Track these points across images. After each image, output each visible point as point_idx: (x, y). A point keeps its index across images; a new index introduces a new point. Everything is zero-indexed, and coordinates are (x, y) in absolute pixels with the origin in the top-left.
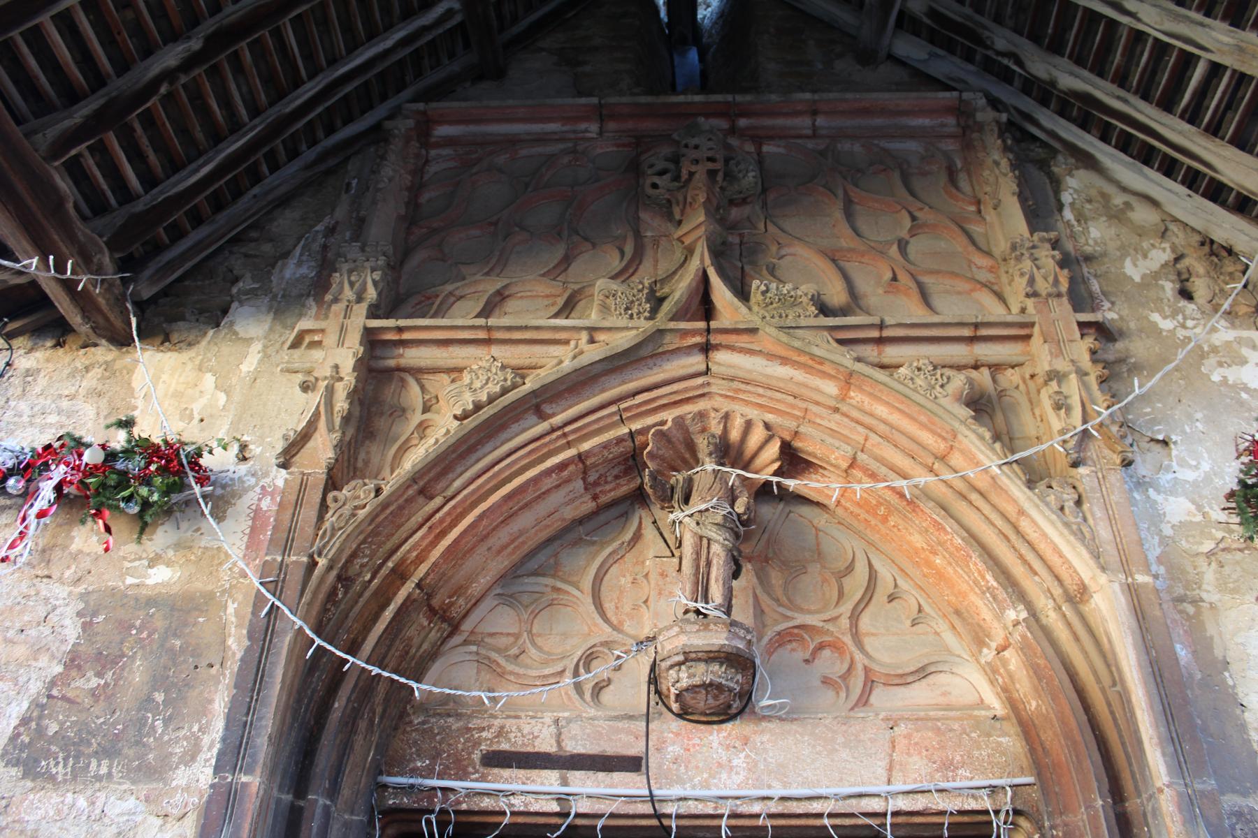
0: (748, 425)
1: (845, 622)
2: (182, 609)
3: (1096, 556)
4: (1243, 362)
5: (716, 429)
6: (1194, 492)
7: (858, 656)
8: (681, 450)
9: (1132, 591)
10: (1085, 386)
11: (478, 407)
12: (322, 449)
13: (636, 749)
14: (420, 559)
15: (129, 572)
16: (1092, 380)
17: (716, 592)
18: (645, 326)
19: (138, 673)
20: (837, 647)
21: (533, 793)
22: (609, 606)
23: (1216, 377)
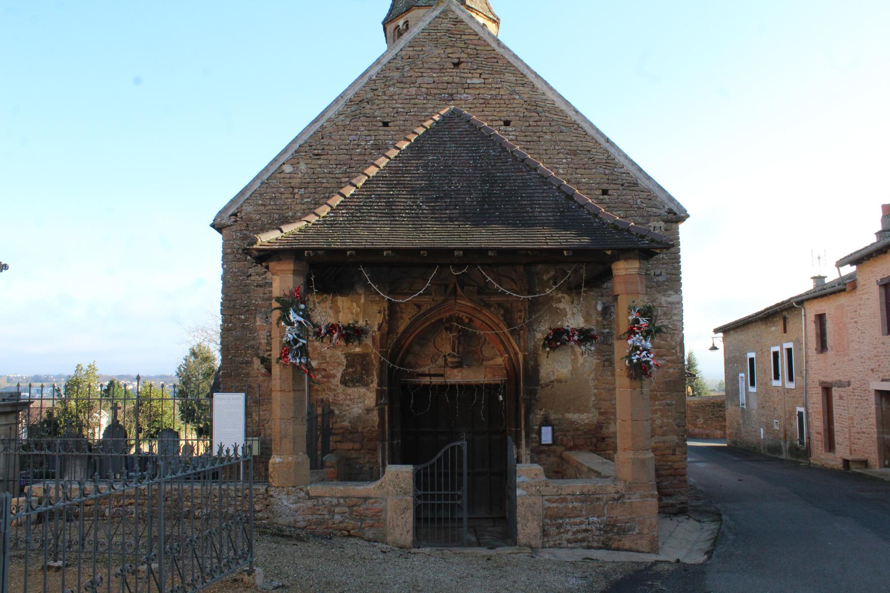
2: (364, 356)
4: (560, 302)
8: (450, 319)
12: (386, 328)
13: (442, 372)
19: (359, 368)
21: (426, 380)
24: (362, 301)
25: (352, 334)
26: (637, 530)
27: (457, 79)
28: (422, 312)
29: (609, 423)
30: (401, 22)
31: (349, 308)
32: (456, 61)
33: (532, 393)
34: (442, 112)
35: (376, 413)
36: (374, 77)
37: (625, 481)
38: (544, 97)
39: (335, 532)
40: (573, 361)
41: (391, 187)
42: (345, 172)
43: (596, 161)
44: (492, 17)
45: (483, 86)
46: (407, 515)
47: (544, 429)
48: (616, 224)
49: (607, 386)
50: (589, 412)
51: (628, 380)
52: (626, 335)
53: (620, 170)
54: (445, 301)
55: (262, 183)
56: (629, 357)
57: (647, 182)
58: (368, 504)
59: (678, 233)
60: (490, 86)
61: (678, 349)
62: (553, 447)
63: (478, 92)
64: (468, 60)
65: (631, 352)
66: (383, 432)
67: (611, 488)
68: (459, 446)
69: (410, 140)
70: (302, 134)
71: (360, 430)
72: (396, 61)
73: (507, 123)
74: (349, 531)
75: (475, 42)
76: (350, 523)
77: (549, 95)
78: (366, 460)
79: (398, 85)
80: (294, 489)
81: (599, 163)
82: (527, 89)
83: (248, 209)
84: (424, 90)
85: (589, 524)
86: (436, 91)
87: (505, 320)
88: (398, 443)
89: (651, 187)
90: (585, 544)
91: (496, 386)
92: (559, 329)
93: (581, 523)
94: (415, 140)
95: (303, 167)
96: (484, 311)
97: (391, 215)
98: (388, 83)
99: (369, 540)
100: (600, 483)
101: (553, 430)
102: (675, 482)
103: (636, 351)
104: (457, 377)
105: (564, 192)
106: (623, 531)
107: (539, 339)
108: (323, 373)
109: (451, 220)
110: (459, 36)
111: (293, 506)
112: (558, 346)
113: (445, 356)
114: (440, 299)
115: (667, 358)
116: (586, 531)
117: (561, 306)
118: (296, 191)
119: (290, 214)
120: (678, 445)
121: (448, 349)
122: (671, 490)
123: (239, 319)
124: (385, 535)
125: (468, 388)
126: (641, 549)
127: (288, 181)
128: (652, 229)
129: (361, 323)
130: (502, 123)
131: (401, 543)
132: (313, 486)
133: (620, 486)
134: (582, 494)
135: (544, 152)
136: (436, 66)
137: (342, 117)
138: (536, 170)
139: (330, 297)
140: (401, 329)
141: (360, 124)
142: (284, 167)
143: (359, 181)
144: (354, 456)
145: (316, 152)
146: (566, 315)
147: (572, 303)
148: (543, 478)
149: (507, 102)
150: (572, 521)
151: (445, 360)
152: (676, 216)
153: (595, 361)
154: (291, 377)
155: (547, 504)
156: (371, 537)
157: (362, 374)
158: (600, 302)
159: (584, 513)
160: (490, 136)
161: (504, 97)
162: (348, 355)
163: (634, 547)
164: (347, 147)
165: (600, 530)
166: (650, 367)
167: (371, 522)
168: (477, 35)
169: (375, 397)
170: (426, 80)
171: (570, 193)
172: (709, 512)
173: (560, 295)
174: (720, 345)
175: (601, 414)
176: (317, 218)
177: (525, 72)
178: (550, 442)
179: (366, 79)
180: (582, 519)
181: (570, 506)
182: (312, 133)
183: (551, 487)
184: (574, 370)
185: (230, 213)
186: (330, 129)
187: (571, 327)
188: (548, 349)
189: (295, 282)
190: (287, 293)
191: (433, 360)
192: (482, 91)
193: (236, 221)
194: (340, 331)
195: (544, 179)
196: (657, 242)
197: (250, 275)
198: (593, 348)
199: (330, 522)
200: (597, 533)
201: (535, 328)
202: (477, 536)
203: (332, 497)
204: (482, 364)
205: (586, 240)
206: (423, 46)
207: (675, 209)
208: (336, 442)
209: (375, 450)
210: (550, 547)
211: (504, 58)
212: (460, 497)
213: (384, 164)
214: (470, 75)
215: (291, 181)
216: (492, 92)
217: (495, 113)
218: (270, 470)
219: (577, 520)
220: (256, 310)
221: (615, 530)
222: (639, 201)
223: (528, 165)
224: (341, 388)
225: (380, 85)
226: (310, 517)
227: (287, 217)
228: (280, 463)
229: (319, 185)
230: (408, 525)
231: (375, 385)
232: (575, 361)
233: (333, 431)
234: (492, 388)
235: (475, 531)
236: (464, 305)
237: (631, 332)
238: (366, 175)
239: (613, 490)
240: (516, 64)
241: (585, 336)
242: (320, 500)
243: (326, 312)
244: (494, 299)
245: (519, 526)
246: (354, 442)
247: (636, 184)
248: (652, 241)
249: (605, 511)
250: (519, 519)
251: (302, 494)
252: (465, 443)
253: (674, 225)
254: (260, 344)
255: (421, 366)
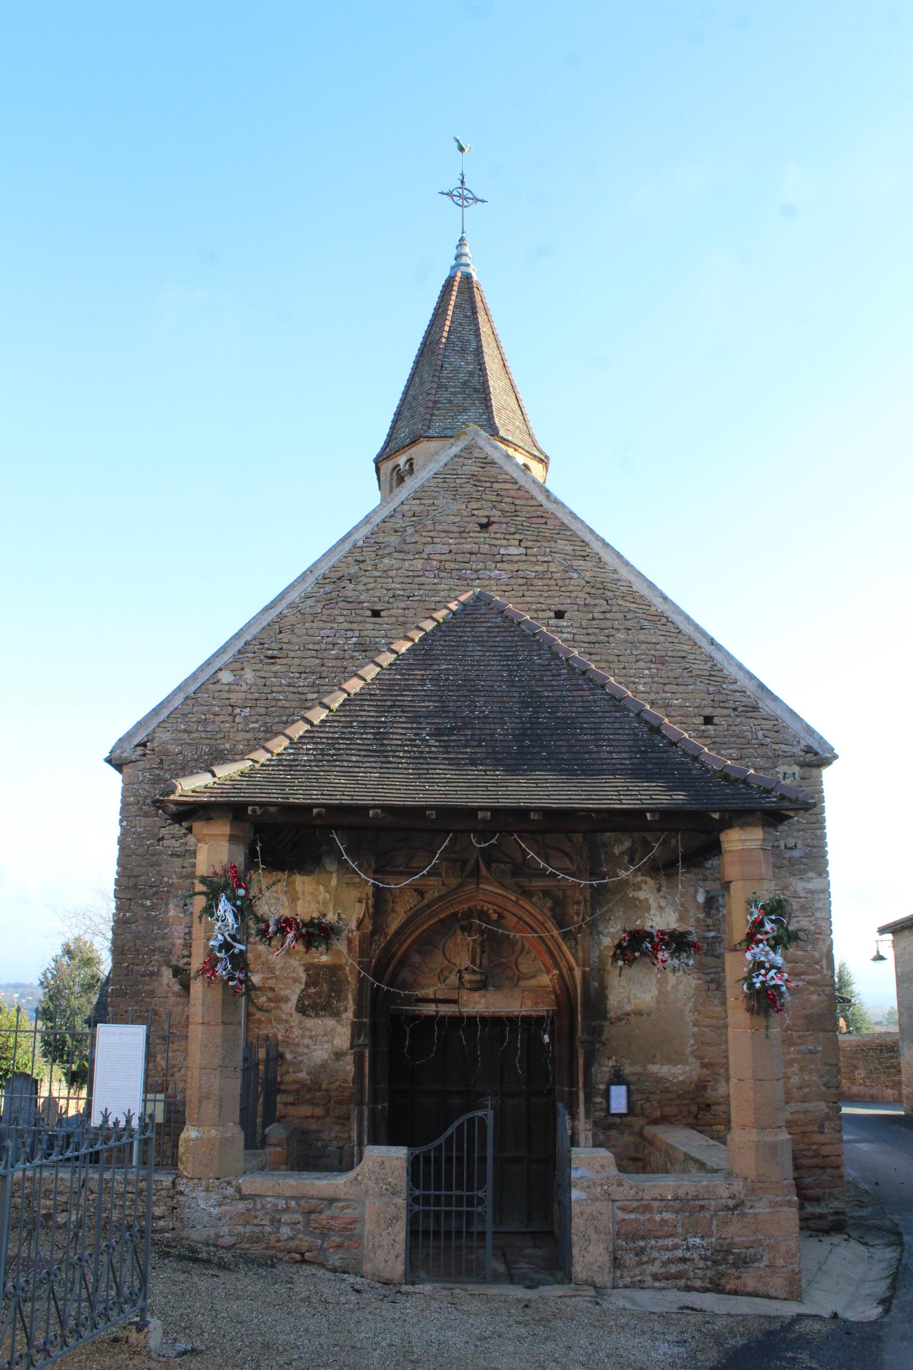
0: (489, 909)
1: (514, 961)
2: (333, 970)
3: (576, 961)
4: (640, 889)
5: (479, 908)
6: (613, 936)
7: (517, 972)
8: (468, 914)
9: (584, 973)
10: (585, 906)
11: (411, 909)
12: (369, 926)
13: (456, 997)
14: (396, 953)
15: (314, 958)
16: (588, 904)
17: (478, 962)
18: (459, 880)
20: (512, 969)
21: (430, 1009)
22: (447, 954)
23: (631, 895)
24: (334, 882)
25: (316, 933)
26: (766, 1261)
27: (485, 548)
28: (425, 902)
29: (717, 1081)
30: (402, 460)
31: (312, 894)
32: (485, 521)
33: (595, 1032)
34: (462, 598)
35: (350, 1058)
36: (360, 543)
37: (745, 1179)
38: (616, 576)
39: (280, 1255)
40: (659, 981)
41: (382, 710)
42: (313, 685)
43: (694, 673)
44: (537, 453)
45: (524, 558)
46: (396, 1230)
47: (614, 1090)
48: (726, 771)
49: (714, 1021)
50: (685, 1062)
51: (748, 1015)
52: (744, 945)
53: (731, 687)
54: (460, 886)
55: (187, 698)
56: (748, 979)
57: (772, 705)
58: (334, 1211)
59: (821, 783)
60: (534, 559)
61: (824, 963)
62: (629, 1119)
63: (516, 567)
64: (503, 519)
65: (751, 971)
66: (361, 1090)
67: (722, 1190)
68: (479, 1118)
69: (413, 640)
70: (249, 625)
71: (324, 1086)
72: (393, 520)
73: (559, 615)
74: (302, 1254)
75: (513, 493)
76: (305, 1241)
77: (624, 572)
78: (333, 1134)
79: (396, 555)
80: (217, 1183)
81: (699, 676)
82: (590, 564)
83: (164, 735)
84: (435, 563)
85: (688, 1249)
86: (452, 565)
87: (554, 916)
88: (383, 1108)
89: (779, 712)
90: (682, 1282)
91: (540, 1020)
92: (637, 932)
93: (676, 1247)
94: (421, 640)
95: (249, 675)
96: (521, 902)
97: (382, 753)
98: (380, 552)
99: (334, 1270)
100: (704, 1181)
101: (629, 1091)
102: (825, 1177)
103: (759, 969)
104: (478, 1004)
105: (646, 722)
106: (743, 1262)
107: (607, 948)
108: (270, 994)
109: (473, 762)
110: (488, 485)
111: (215, 1211)
112: (635, 958)
113: (459, 971)
114: (453, 882)
115: (807, 978)
116: (684, 1260)
117: (641, 895)
118: (238, 711)
119: (227, 746)
120: (828, 1118)
121: (464, 960)
122: (817, 1192)
123: (143, 905)
124: (360, 1263)
125: (496, 1022)
126: (772, 1292)
127: (226, 695)
128: (781, 776)
129: (331, 917)
130: (552, 614)
131: (387, 1275)
132: (247, 1178)
133: (738, 1186)
134: (675, 1199)
135: (616, 659)
136: (455, 529)
137: (310, 602)
138: (603, 687)
139: (284, 876)
140: (393, 927)
141: (337, 612)
142: (221, 675)
143: (334, 701)
144: (314, 1126)
145: (270, 653)
146: (648, 909)
147: (659, 890)
148: (615, 1171)
149: (560, 583)
150: (661, 1242)
151: (461, 978)
152: (817, 757)
153: (694, 982)
154: (220, 1004)
155: (621, 1215)
156: (337, 1264)
157: (330, 996)
158: (701, 890)
159: (680, 1230)
160: (535, 635)
161: (555, 575)
162: (308, 968)
163: (761, 1289)
164: (317, 647)
165: (705, 1259)
166: (781, 994)
167: (338, 1240)
168: (516, 483)
169: (349, 1033)
170: (438, 548)
171: (655, 723)
172: (879, 1229)
173: (639, 879)
174: (889, 952)
175: (704, 1066)
176: (269, 756)
177: (588, 538)
178: (624, 1110)
179: (348, 546)
180: (677, 1240)
181: (657, 1218)
182: (264, 624)
183: (626, 1187)
184: (662, 996)
185: (136, 741)
186: (292, 619)
187: (658, 928)
188: (620, 963)
189: (231, 855)
190: (219, 870)
191: (442, 978)
192: (522, 566)
193: (144, 755)
194: (298, 929)
195: (617, 702)
196: (790, 800)
197: (163, 839)
198: (691, 962)
199: (273, 1238)
200: (701, 1265)
201: (601, 928)
202: (506, 1262)
203: (278, 1197)
204: (517, 985)
205: (680, 797)
206: (435, 498)
207: (816, 746)
208: (286, 1104)
209: (348, 1119)
210: (626, 1287)
211: (556, 518)
212: (481, 1201)
213: (373, 675)
214: (504, 542)
215: (230, 696)
216: (537, 568)
217: (542, 600)
218: (181, 1150)
219: (669, 1242)
220: (168, 892)
221: (731, 1259)
222: (760, 734)
223: (591, 680)
224: (296, 1018)
225: (368, 555)
226: (241, 1229)
227: (222, 751)
228: (197, 1139)
229: (274, 703)
230: (397, 1246)
231: (349, 1015)
232: (662, 982)
233: (282, 1087)
234: (532, 1024)
235: (504, 1255)
236: (491, 893)
237: (751, 939)
238: (344, 691)
239: (725, 1194)
240: (574, 526)
241: (677, 942)
242: (258, 1200)
243: (278, 899)
244: (538, 883)
245: (575, 1251)
246: (313, 1104)
247: (756, 708)
248: (783, 797)
249: (714, 1227)
250: (575, 1238)
251: (230, 1191)
252: (490, 1113)
253: (814, 771)
254: (173, 945)
255: (422, 987)
